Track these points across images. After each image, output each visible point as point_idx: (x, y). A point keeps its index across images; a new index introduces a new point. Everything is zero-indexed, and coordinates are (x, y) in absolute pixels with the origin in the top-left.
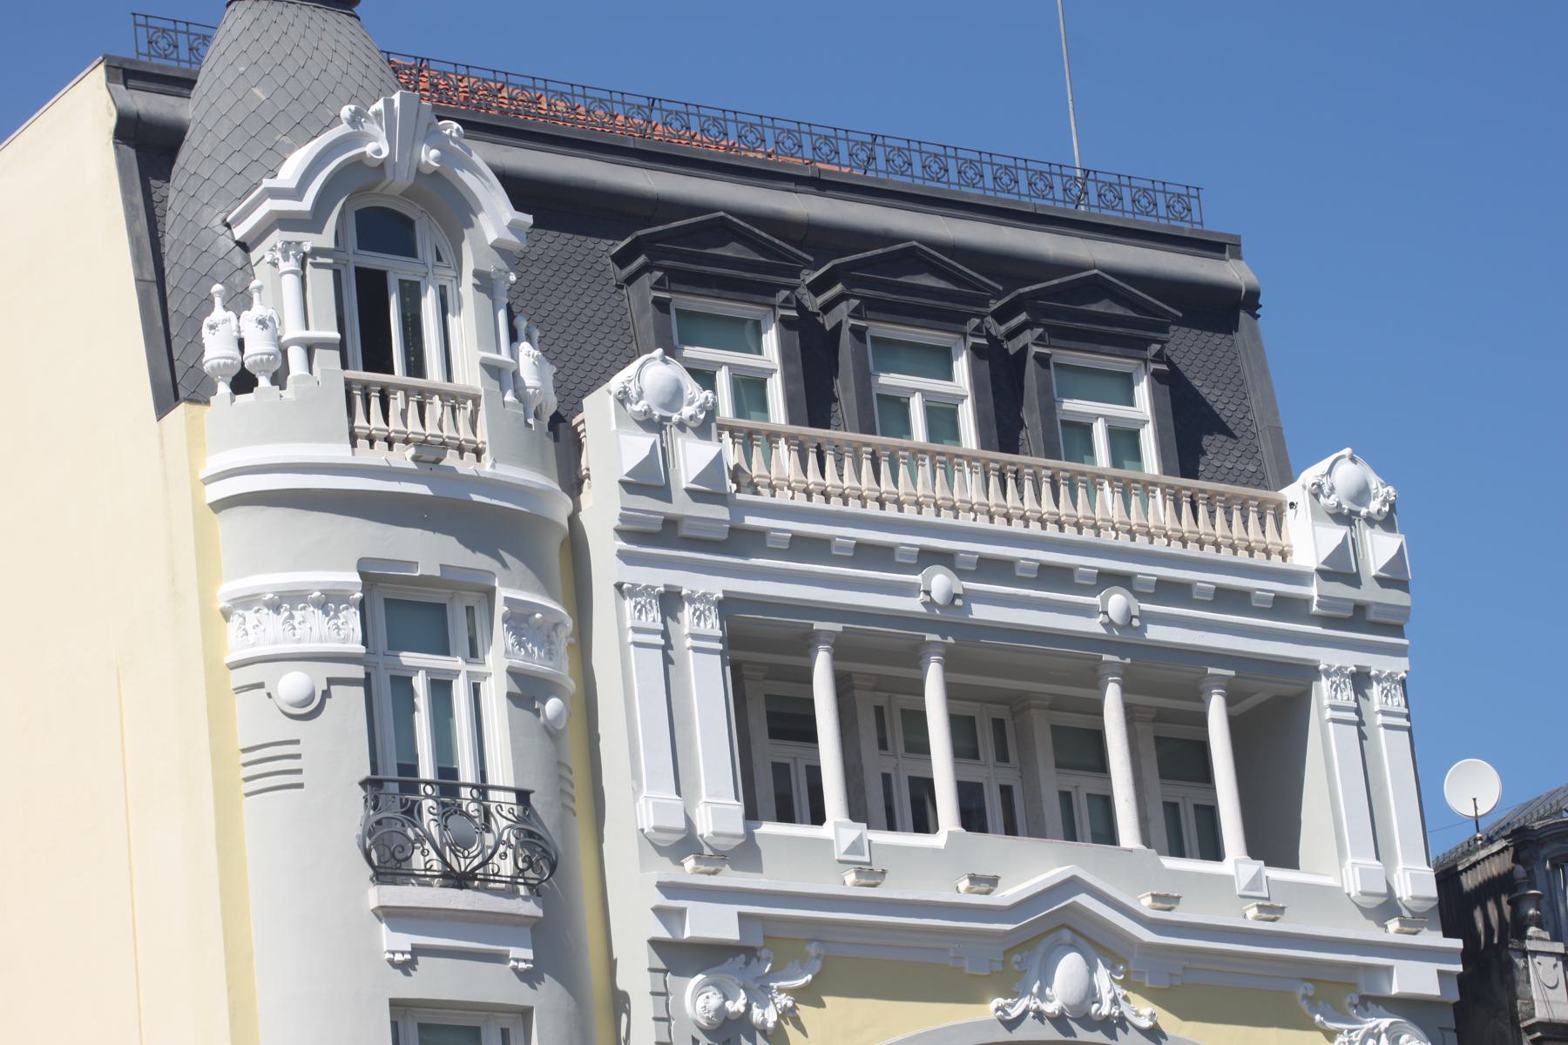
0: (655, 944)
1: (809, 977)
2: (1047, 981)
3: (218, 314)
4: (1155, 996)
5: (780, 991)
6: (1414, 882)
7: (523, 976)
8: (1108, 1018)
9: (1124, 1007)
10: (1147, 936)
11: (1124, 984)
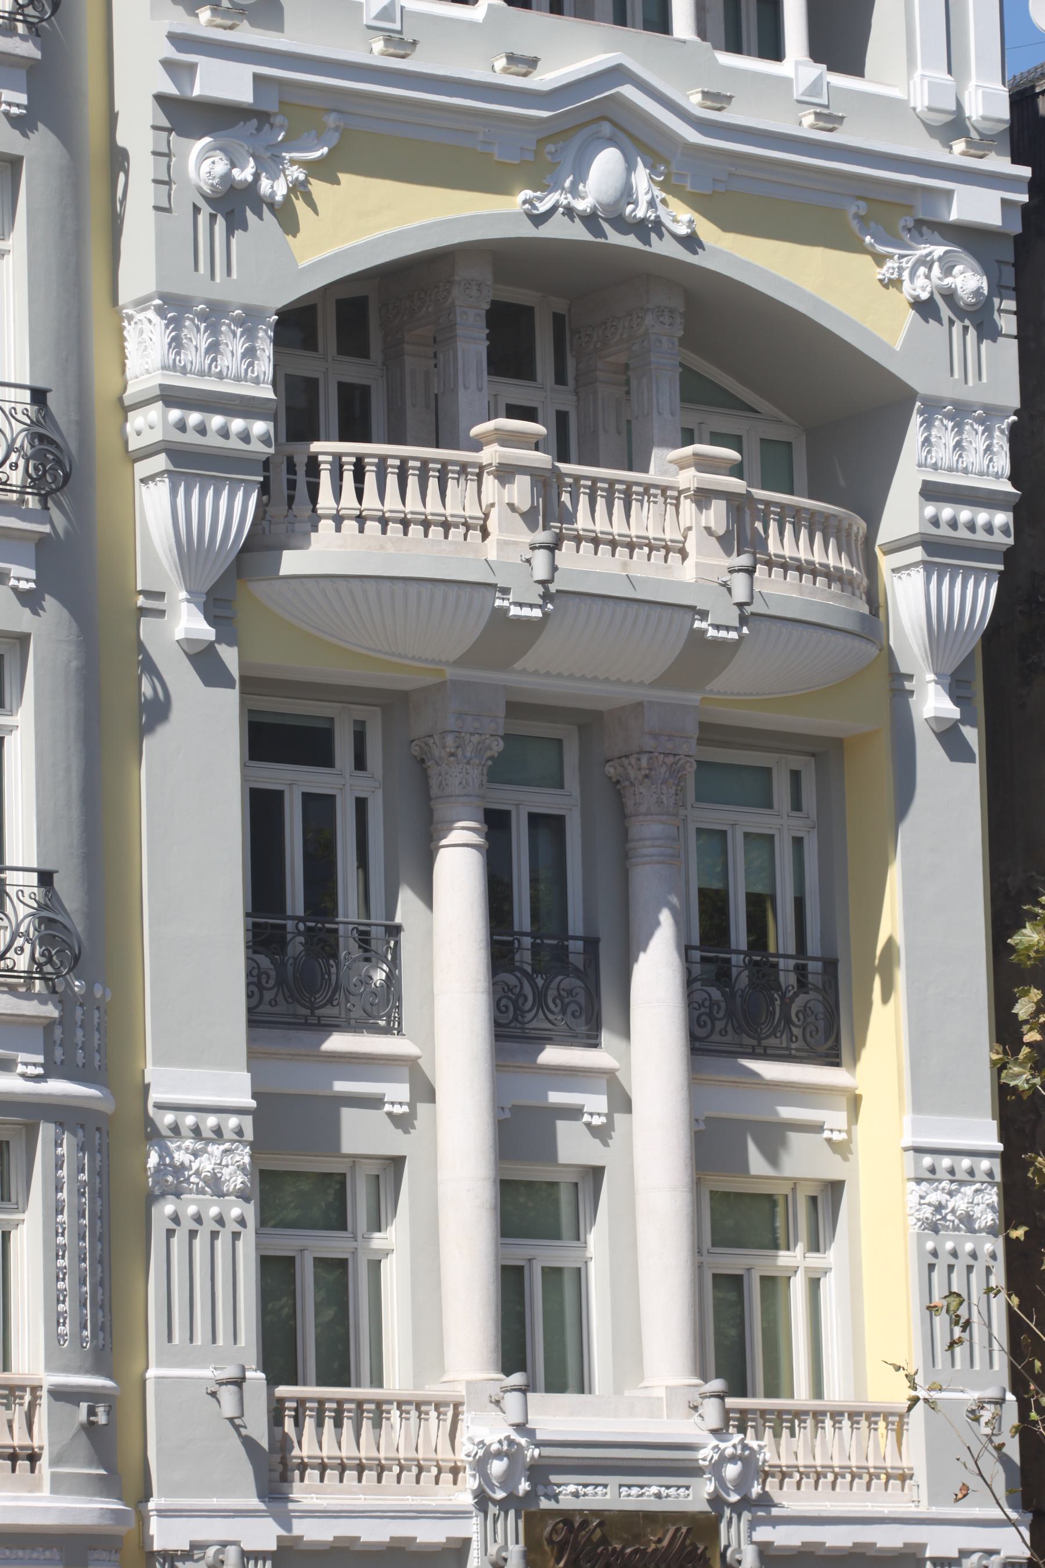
0: (161, 99)
1: (325, 150)
2: (581, 174)
4: (698, 202)
5: (293, 162)
6: (987, 101)
7: (15, 122)
8: (643, 221)
9: (661, 211)
10: (693, 136)
11: (664, 186)
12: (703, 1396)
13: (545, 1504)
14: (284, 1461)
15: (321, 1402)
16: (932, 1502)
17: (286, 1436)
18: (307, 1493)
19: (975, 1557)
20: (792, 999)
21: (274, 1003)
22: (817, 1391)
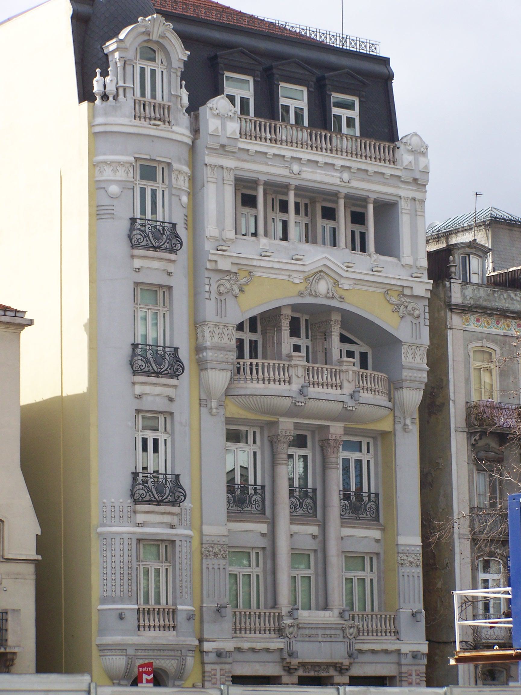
3: (98, 77)
20: (367, 504)
21: (233, 507)
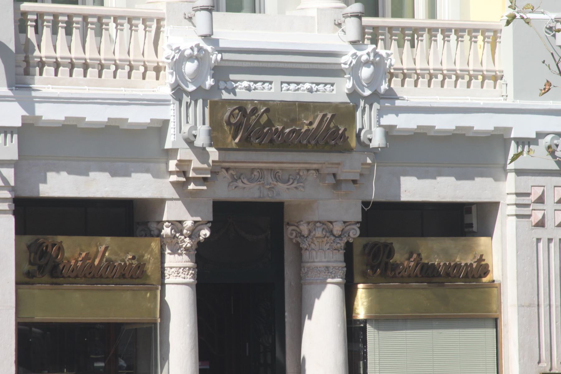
12: (346, 16)
13: (226, 96)
14: (27, 60)
15: (56, 16)
16: (516, 97)
17: (28, 40)
18: (44, 84)
19: (548, 138)
22: (432, 13)
